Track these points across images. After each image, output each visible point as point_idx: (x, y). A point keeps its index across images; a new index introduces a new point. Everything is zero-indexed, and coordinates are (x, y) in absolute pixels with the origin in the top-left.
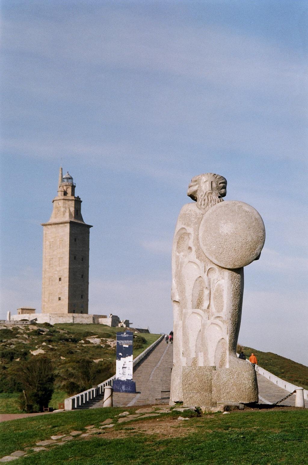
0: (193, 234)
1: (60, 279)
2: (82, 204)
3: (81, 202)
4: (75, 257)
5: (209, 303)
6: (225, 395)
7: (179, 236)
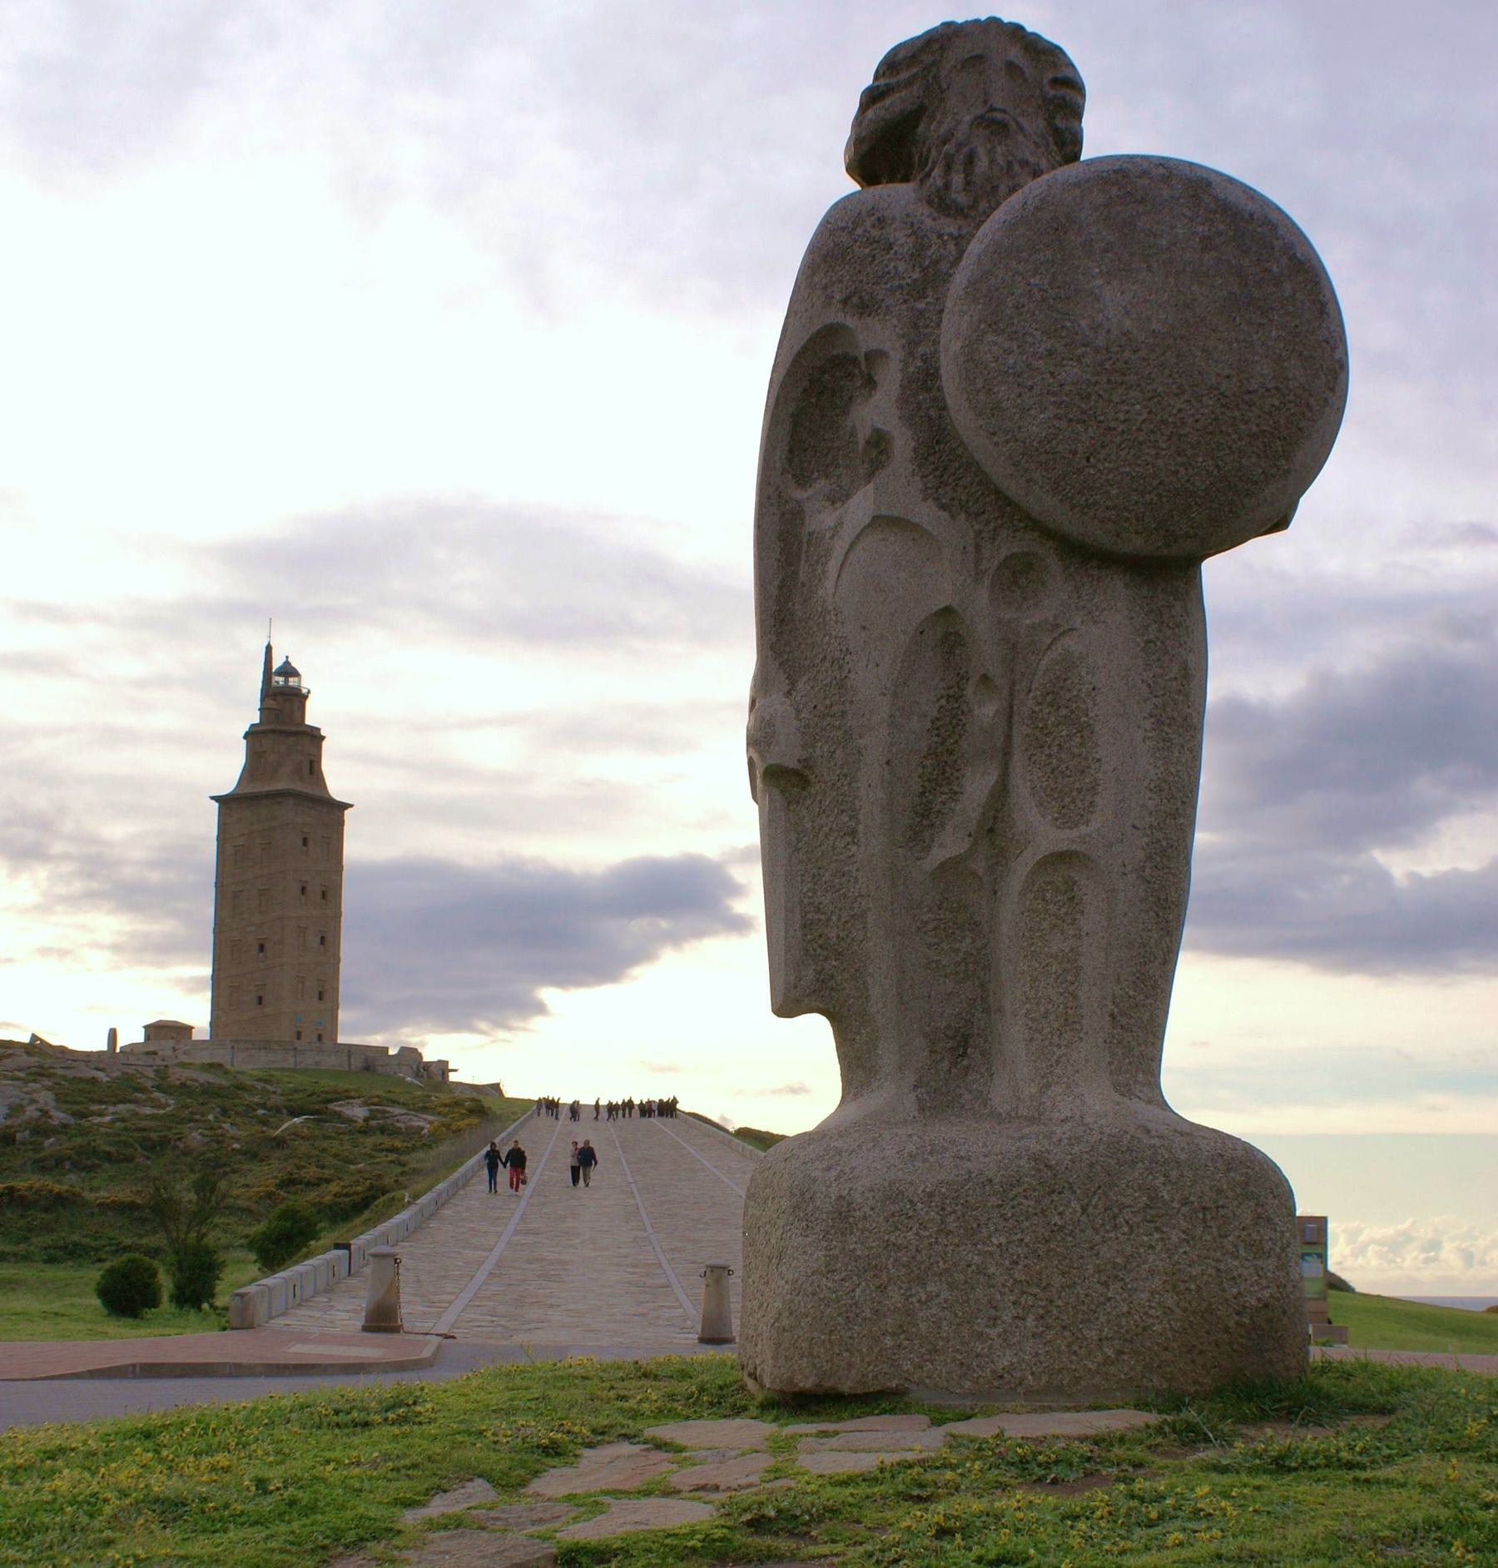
0: (896, 356)
1: (262, 948)
2: (324, 744)
3: (323, 738)
4: (303, 889)
5: (992, 778)
6: (1110, 1352)
7: (806, 383)
